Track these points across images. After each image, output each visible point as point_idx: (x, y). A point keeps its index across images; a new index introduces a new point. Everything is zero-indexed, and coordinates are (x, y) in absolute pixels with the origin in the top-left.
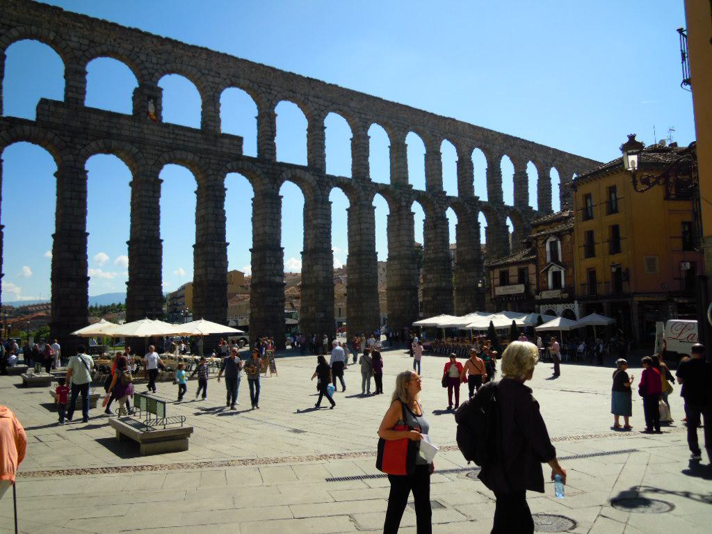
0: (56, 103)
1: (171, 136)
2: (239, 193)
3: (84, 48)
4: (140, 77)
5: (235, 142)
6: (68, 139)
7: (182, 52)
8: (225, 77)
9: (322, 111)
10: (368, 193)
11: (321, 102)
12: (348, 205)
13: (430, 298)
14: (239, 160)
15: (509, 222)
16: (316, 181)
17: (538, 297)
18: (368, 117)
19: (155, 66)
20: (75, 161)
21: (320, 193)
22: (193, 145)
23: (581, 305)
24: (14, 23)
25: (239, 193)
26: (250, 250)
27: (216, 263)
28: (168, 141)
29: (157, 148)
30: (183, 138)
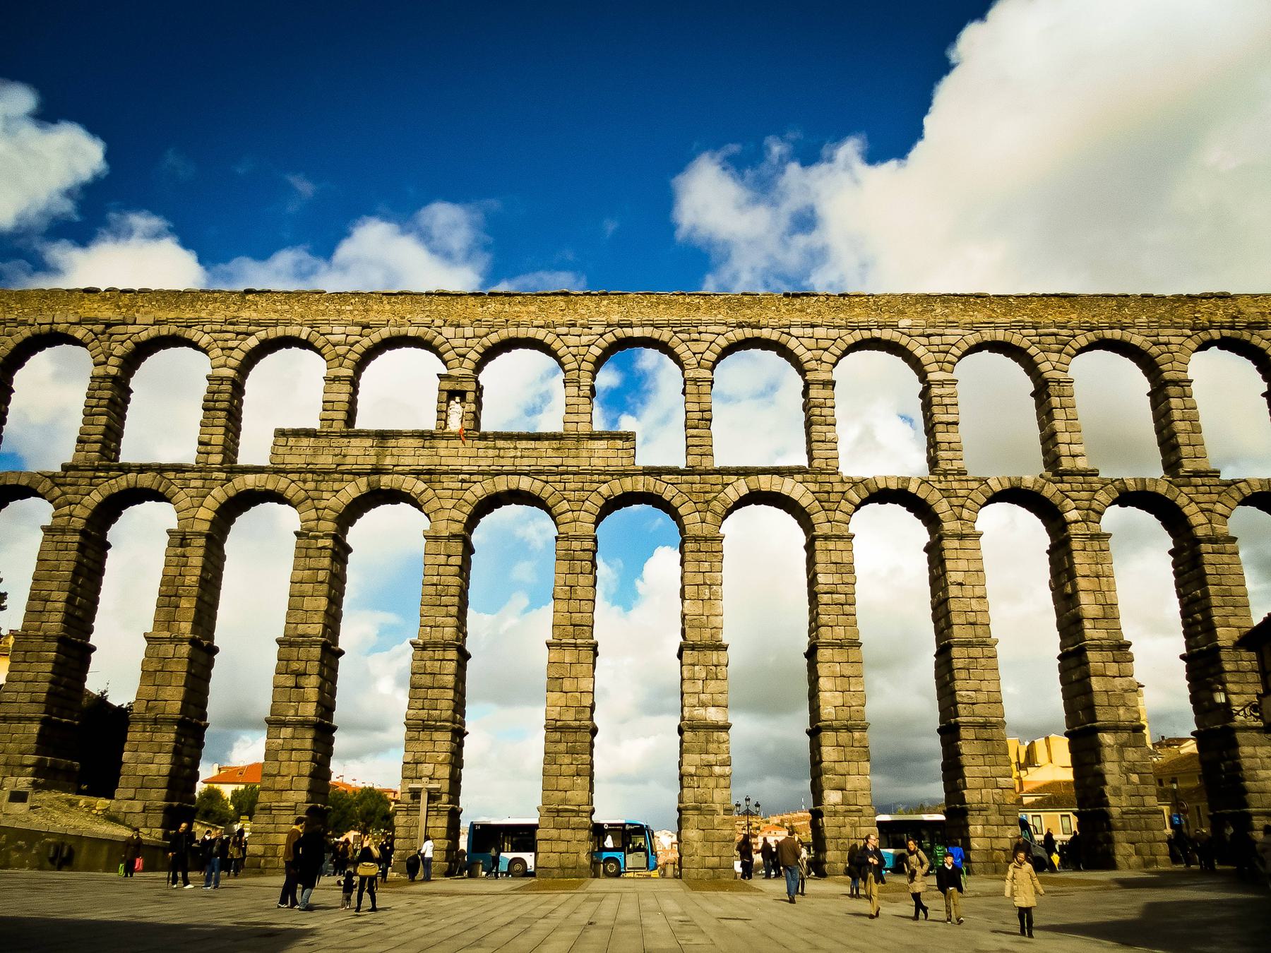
0: (297, 433)
1: (491, 453)
3: (351, 339)
5: (619, 443)
6: (311, 485)
8: (600, 330)
9: (826, 350)
10: (960, 501)
14: (627, 475)
18: (952, 340)
20: (319, 519)
22: (533, 462)
24: (252, 328)
27: (567, 684)
28: (483, 462)
29: (461, 477)
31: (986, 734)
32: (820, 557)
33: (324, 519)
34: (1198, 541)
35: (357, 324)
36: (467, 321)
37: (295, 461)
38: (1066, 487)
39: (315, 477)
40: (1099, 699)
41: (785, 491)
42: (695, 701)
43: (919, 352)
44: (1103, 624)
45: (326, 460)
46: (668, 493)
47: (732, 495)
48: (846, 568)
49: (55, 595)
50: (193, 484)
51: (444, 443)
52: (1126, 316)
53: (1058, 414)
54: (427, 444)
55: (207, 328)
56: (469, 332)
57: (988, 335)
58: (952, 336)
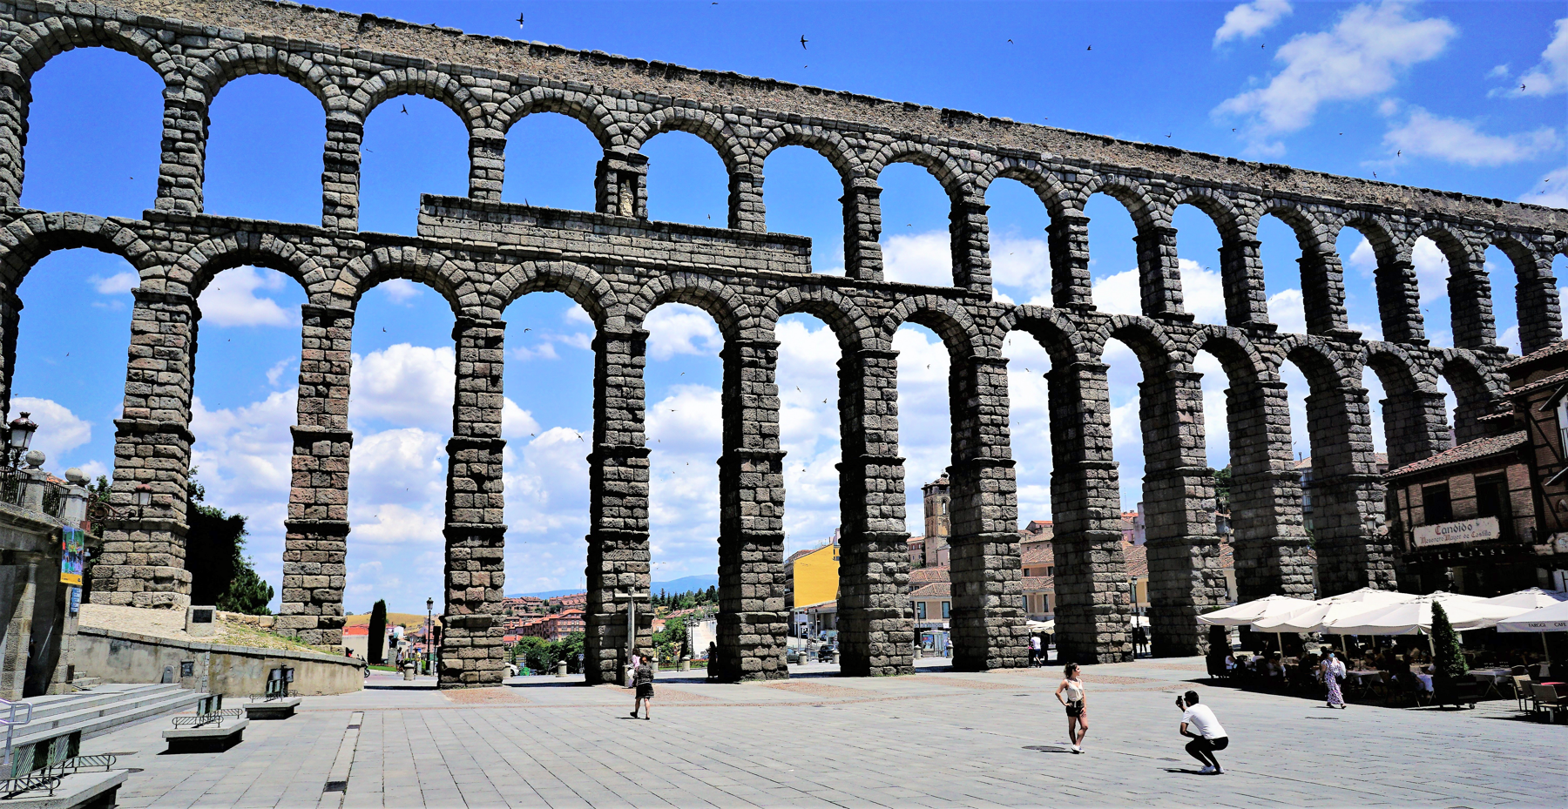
1: (667, 244)
2: (806, 349)
4: (606, 140)
6: (471, 265)
9: (979, 173)
12: (1048, 366)
13: (1251, 563)
15: (1442, 385)
16: (963, 321)
18: (1081, 178)
25: (806, 349)
26: (838, 466)
27: (763, 494)
31: (1110, 545)
32: (981, 379)
33: (489, 305)
35: (503, 78)
38: (1170, 329)
40: (1191, 516)
42: (877, 512)
43: (1058, 186)
45: (484, 236)
47: (901, 310)
48: (1000, 391)
49: (164, 377)
50: (325, 251)
53: (1165, 259)
55: (318, 57)
56: (632, 104)
58: (1085, 174)
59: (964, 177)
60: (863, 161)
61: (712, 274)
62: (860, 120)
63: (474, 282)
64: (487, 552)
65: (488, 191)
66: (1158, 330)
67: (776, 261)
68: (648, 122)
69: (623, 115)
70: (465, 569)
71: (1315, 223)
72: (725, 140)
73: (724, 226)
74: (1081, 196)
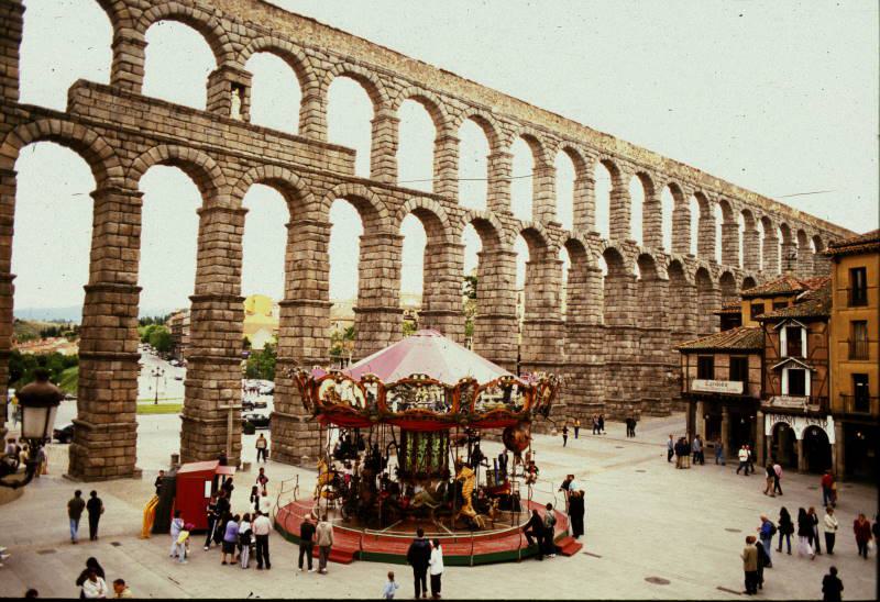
0: (100, 88)
1: (262, 144)
5: (347, 156)
6: (117, 143)
7: (280, 21)
8: (336, 60)
9: (457, 116)
11: (456, 103)
13: (573, 375)
17: (766, 404)
18: (513, 128)
19: (243, 39)
21: (450, 232)
23: (840, 424)
27: (317, 332)
30: (278, 148)
34: (590, 269)
36: (241, 19)
37: (101, 115)
38: (550, 231)
39: (123, 136)
41: (435, 211)
43: (498, 131)
44: (556, 310)
45: (129, 122)
46: (375, 200)
51: (227, 128)
52: (580, 135)
54: (214, 125)
56: (242, 30)
57: (529, 131)
59: (448, 118)
60: (390, 98)
61: (291, 168)
62: (393, 68)
63: (119, 156)
64: (125, 375)
65: (133, 82)
66: (544, 232)
67: (334, 163)
68: (253, 46)
69: (235, 37)
70: (109, 388)
71: (621, 172)
72: (304, 68)
73: (294, 130)
74: (511, 139)
